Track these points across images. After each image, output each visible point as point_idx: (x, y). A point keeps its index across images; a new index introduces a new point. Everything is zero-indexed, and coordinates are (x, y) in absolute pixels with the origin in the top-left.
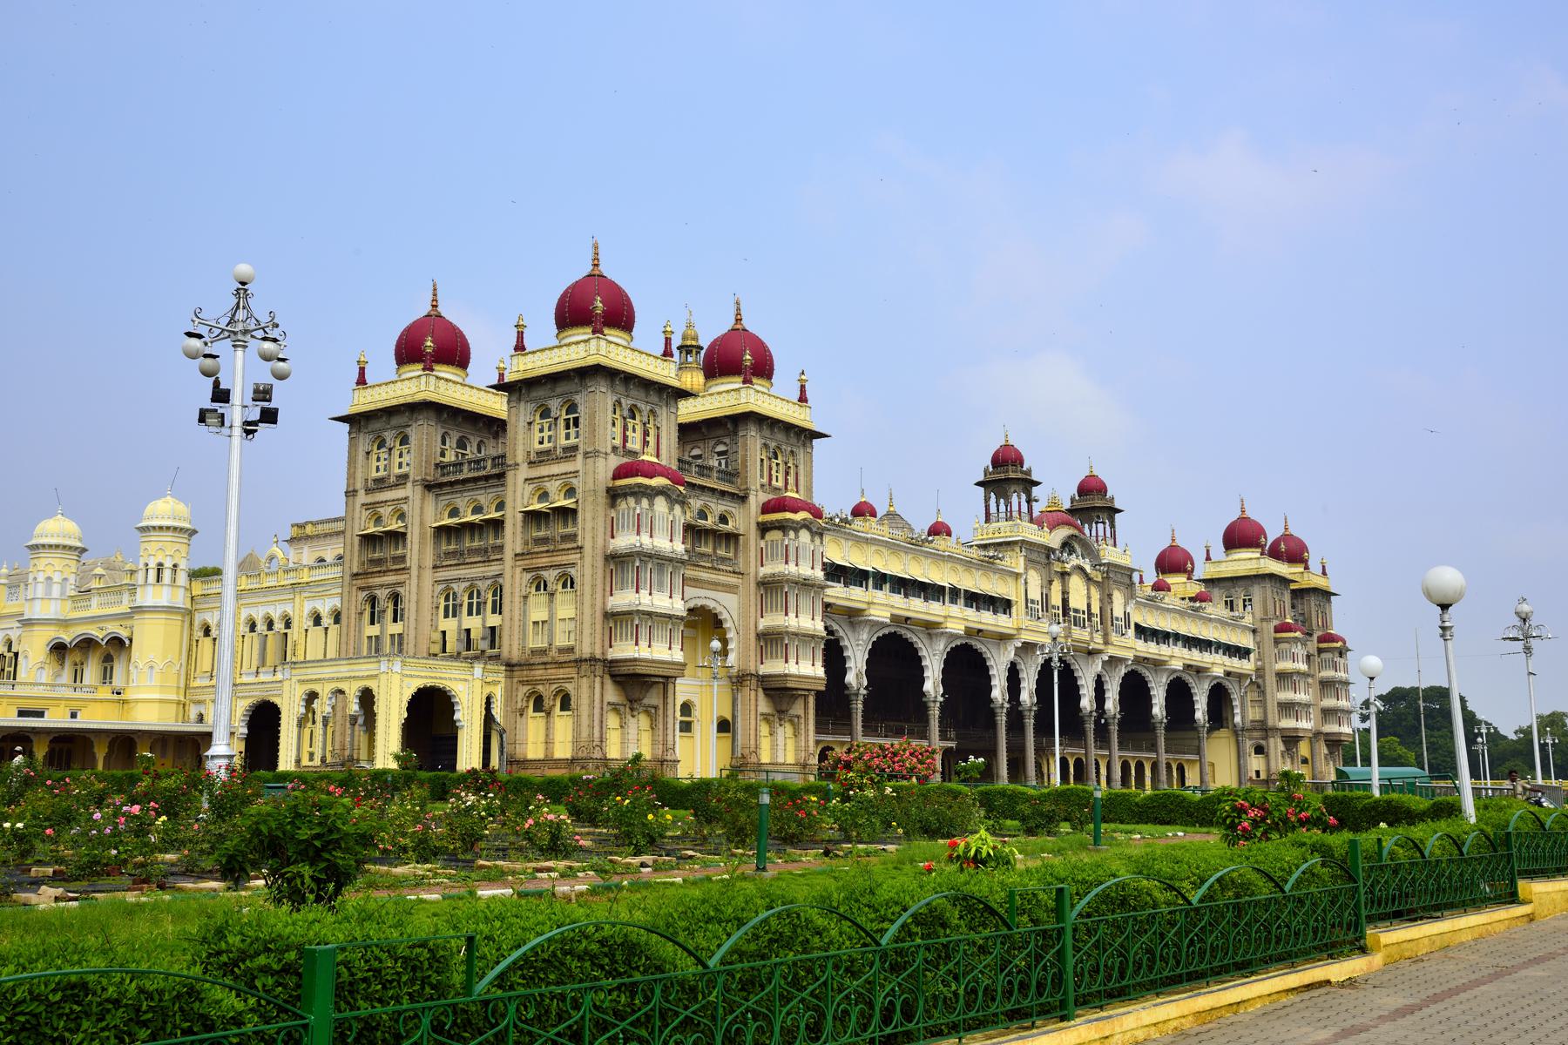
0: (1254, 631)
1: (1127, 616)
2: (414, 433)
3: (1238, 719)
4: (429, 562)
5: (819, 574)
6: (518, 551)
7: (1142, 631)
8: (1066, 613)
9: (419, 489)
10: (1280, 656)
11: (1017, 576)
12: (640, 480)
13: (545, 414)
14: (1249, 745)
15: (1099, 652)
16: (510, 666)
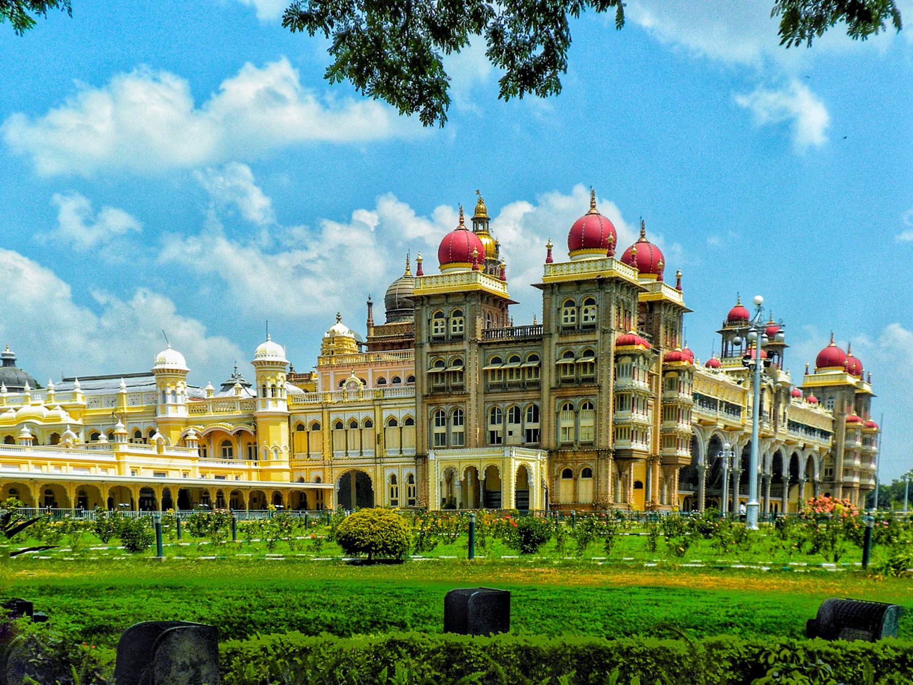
0: (833, 421)
1: (784, 413)
2: (466, 309)
4: (482, 390)
5: (691, 397)
6: (553, 385)
8: (760, 414)
15: (770, 437)
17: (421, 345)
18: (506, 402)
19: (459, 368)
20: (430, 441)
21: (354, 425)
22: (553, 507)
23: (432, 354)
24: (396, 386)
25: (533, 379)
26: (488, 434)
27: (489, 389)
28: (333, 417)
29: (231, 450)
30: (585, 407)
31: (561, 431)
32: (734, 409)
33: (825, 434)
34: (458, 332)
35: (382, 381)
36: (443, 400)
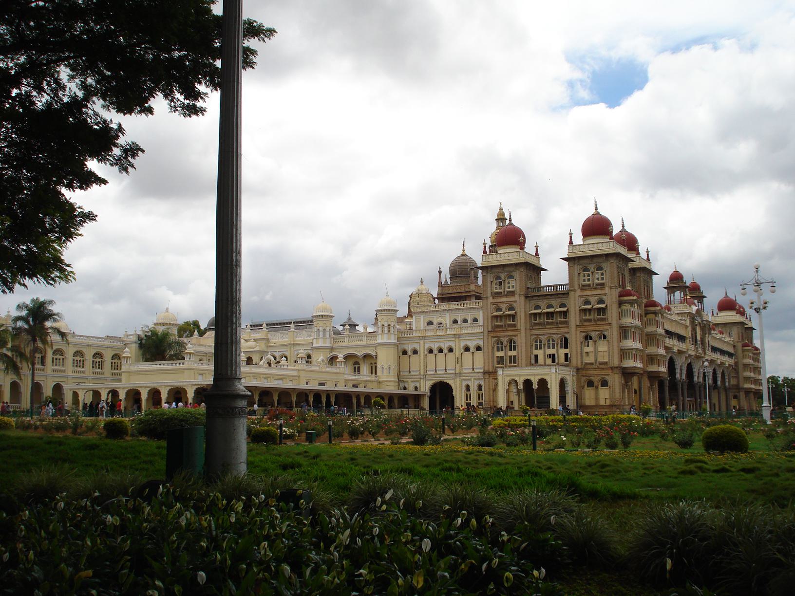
0: (734, 346)
3: (727, 384)
7: (715, 349)
9: (523, 298)
10: (744, 357)
11: (687, 327)
12: (631, 298)
13: (586, 269)
14: (731, 395)
16: (578, 369)
17: (487, 298)
18: (543, 333)
19: (513, 312)
20: (493, 362)
21: (441, 351)
22: (581, 406)
23: (493, 304)
24: (465, 324)
25: (563, 319)
26: (533, 357)
27: (533, 327)
28: (427, 346)
29: (359, 368)
30: (600, 338)
31: (584, 354)
32: (681, 338)
33: (730, 355)
34: (511, 289)
36: (502, 334)
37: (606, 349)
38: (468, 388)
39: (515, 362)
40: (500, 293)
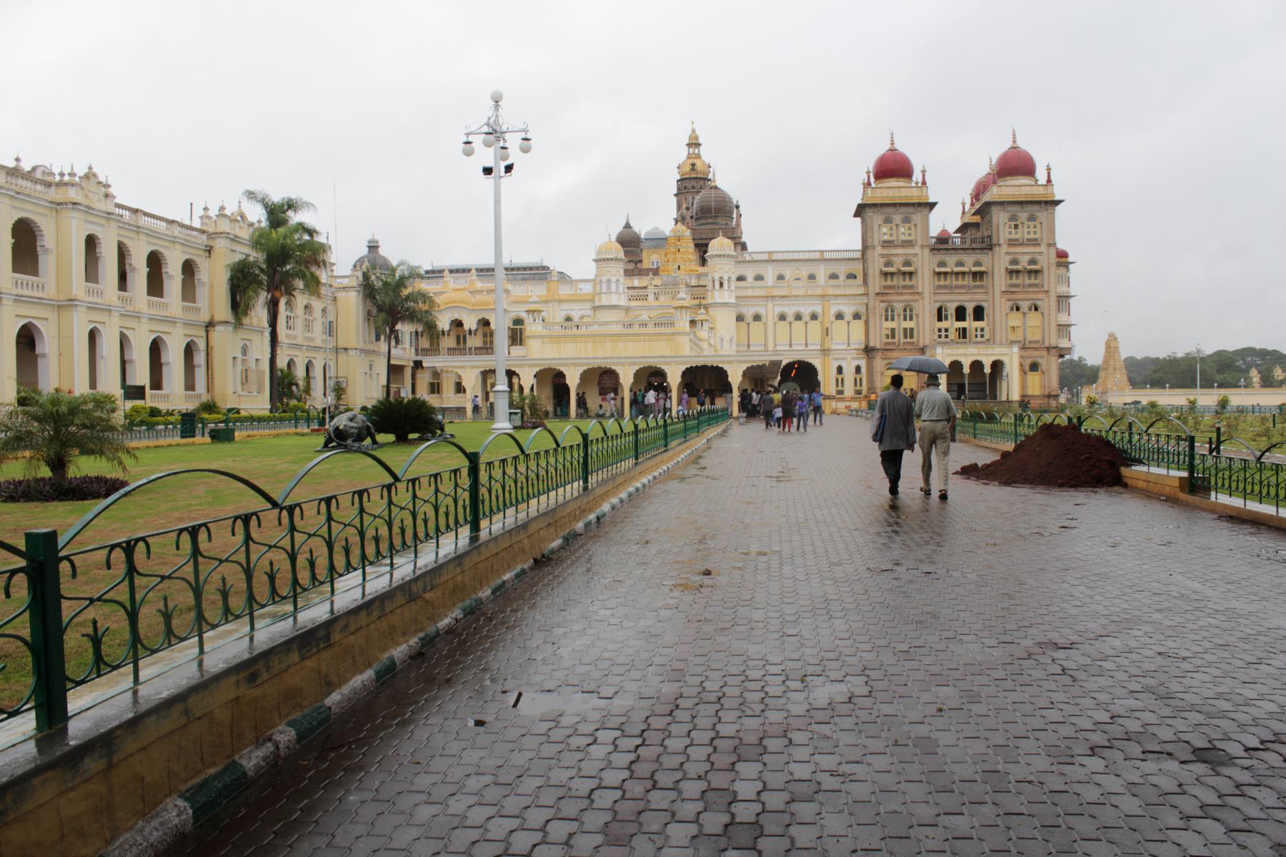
9: (927, 251)
17: (874, 247)
21: (798, 317)
23: (883, 256)
28: (778, 310)
35: (781, 278)
37: (1038, 323)
38: (840, 370)
39: (912, 337)
40: (892, 242)
